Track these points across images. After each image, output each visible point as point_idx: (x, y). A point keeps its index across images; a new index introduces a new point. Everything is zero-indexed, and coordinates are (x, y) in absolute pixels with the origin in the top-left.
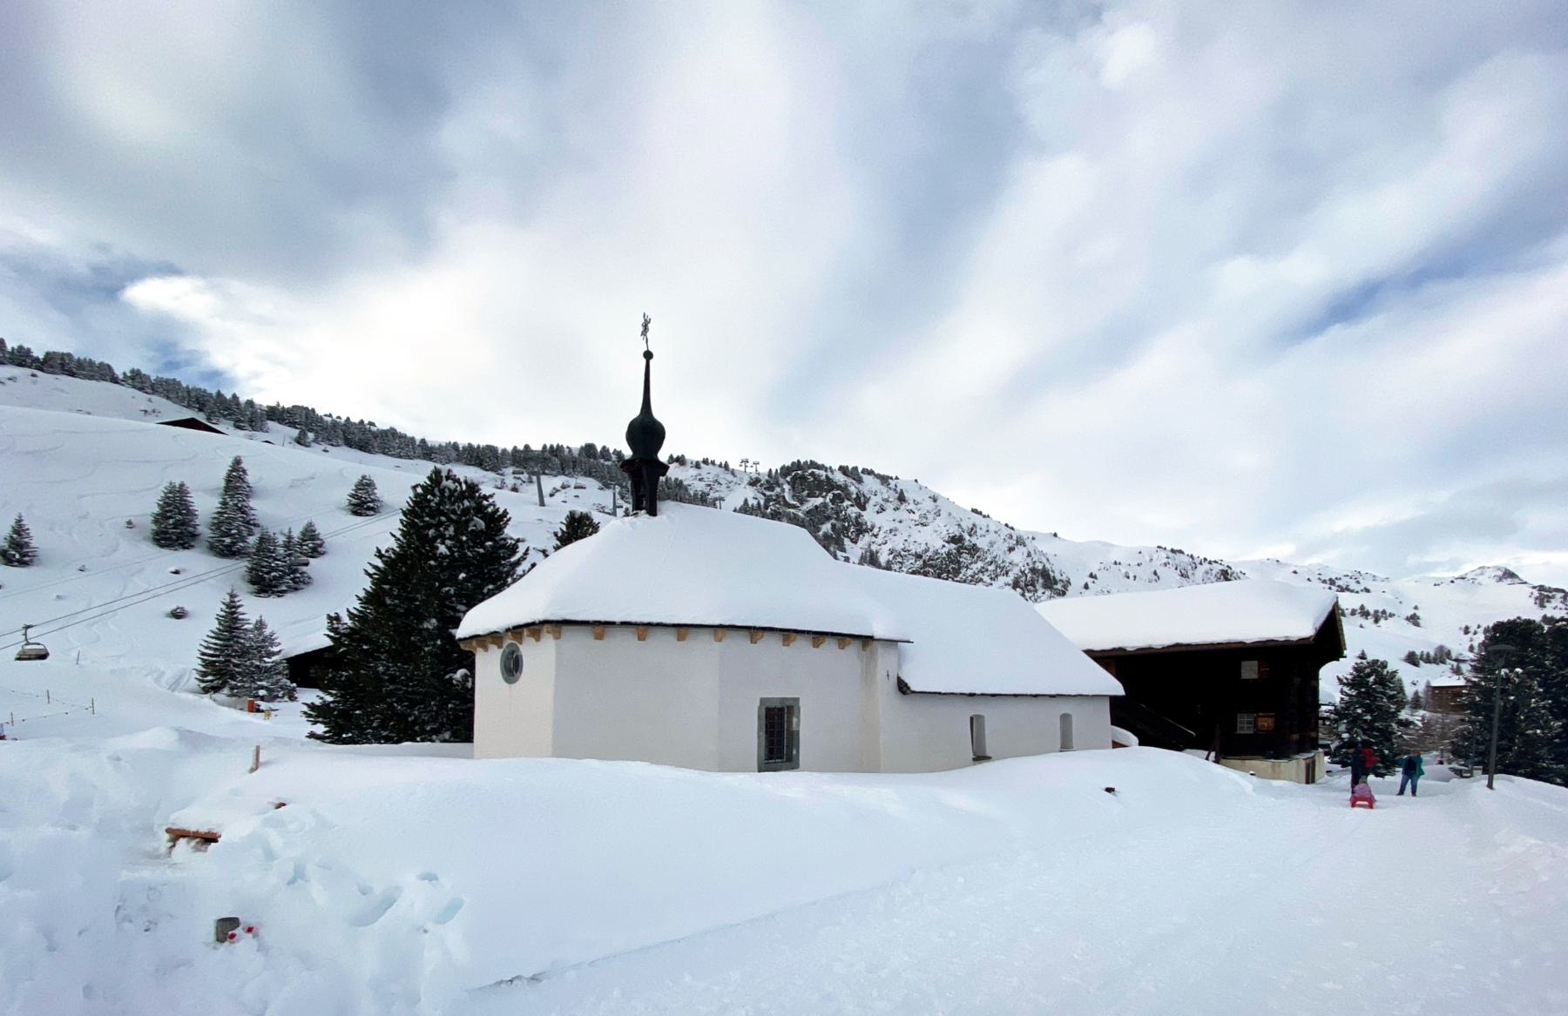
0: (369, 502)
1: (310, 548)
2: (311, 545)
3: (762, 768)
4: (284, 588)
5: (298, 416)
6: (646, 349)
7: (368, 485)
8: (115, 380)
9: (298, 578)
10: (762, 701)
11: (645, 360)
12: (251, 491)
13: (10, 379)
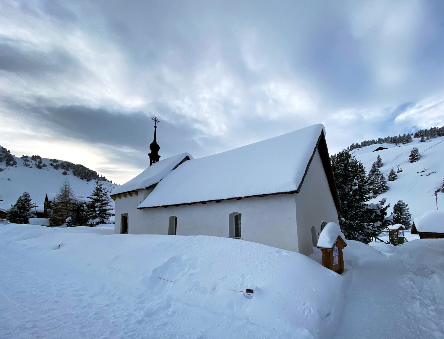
0: (416, 157)
1: (392, 178)
2: (392, 177)
3: (121, 234)
4: (380, 192)
5: (422, 133)
6: (155, 125)
7: (415, 151)
8: (375, 143)
9: (385, 188)
10: (122, 214)
11: (155, 128)
12: (383, 164)
13: (354, 152)
